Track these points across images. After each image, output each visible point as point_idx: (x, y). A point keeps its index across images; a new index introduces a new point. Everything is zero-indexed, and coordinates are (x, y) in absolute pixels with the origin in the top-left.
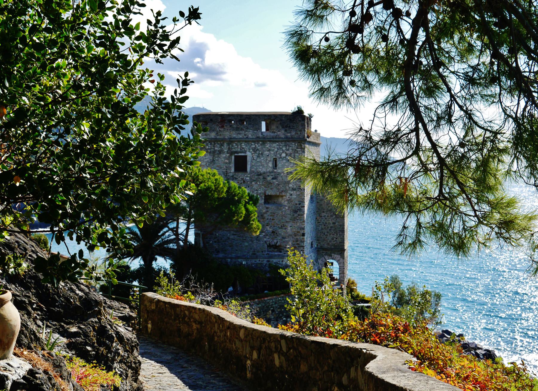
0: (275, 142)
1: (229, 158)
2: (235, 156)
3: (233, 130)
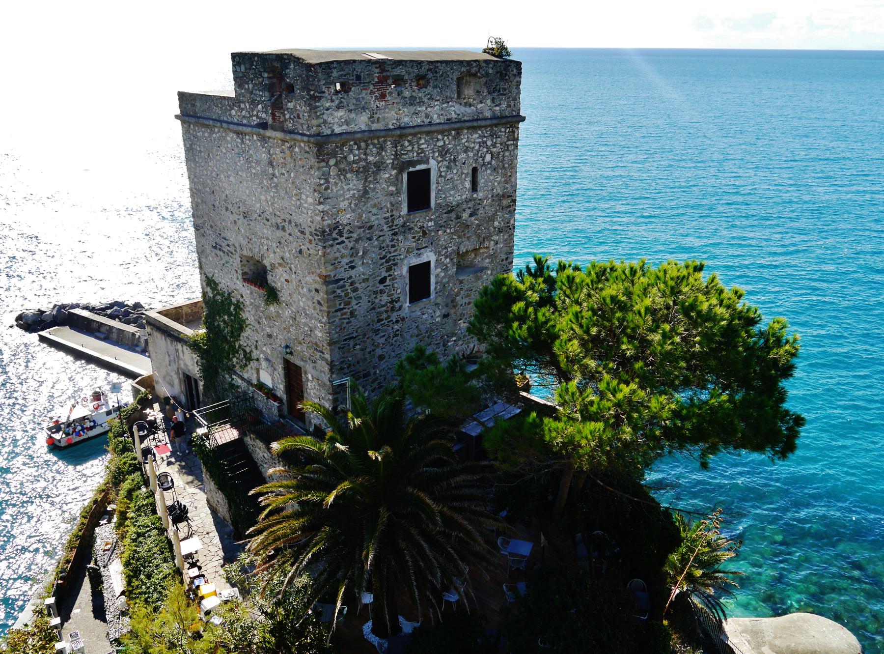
0: (474, 129)
1: (397, 180)
2: (409, 173)
3: (404, 105)
